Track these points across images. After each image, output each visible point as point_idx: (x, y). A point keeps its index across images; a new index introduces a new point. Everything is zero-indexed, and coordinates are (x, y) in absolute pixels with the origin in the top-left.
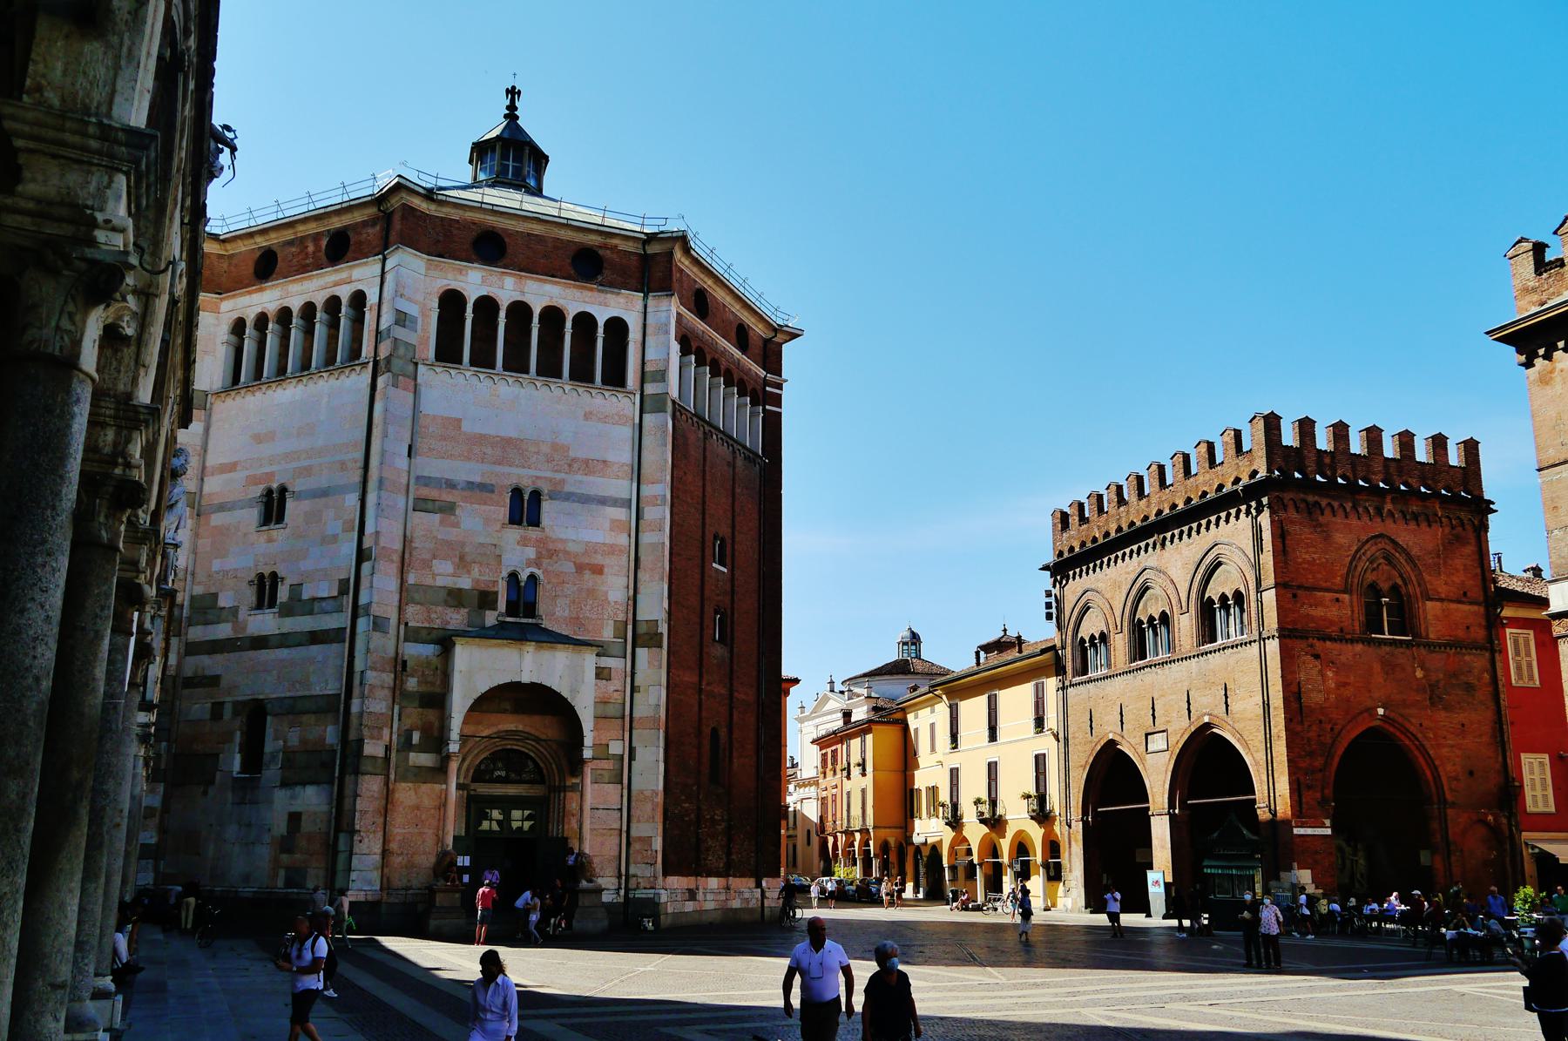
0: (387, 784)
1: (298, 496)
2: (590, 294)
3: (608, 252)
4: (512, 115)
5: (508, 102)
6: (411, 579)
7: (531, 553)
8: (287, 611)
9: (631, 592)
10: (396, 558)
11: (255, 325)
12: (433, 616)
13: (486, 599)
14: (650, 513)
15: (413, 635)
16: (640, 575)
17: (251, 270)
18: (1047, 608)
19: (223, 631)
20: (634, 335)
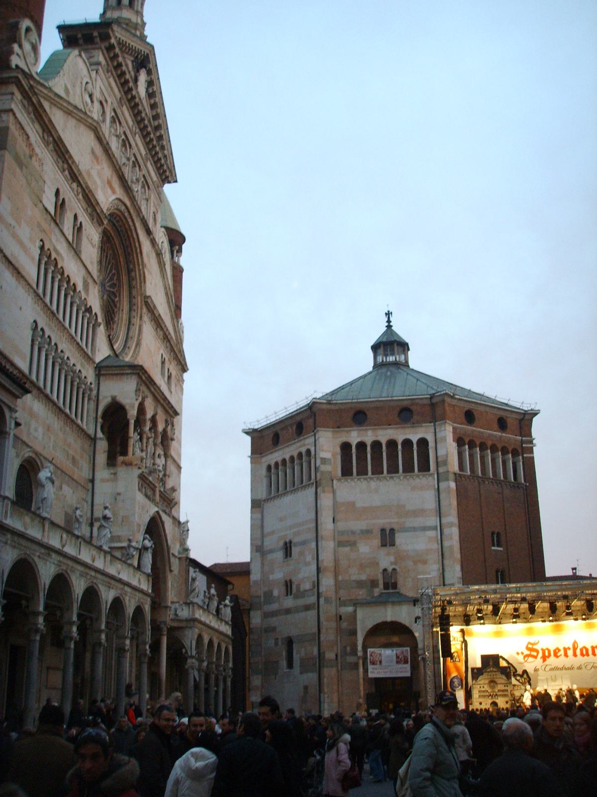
0: (338, 671)
2: (407, 429)
4: (389, 327)
5: (387, 319)
6: (340, 578)
7: (392, 559)
8: (296, 597)
9: (441, 571)
10: (333, 569)
13: (374, 583)
14: (446, 531)
15: (343, 603)
16: (445, 562)
17: (271, 442)
19: (275, 607)
20: (431, 444)
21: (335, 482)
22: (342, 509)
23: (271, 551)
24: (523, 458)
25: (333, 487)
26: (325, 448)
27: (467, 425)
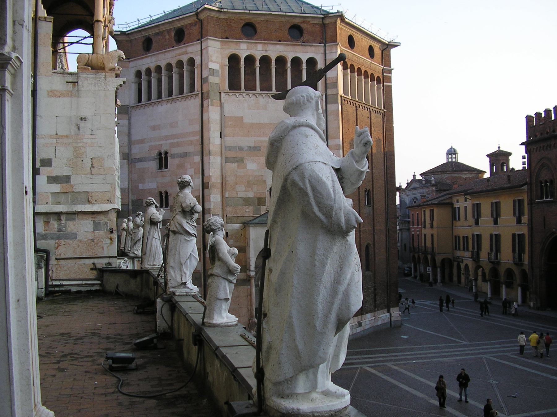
1: (173, 156)
2: (298, 47)
3: (305, 25)
6: (227, 195)
10: (220, 185)
11: (146, 73)
12: (238, 211)
13: (261, 201)
18: (523, 164)
21: (222, 94)
22: (230, 123)
23: (140, 160)
24: (383, 85)
25: (220, 100)
26: (214, 58)
27: (349, 50)
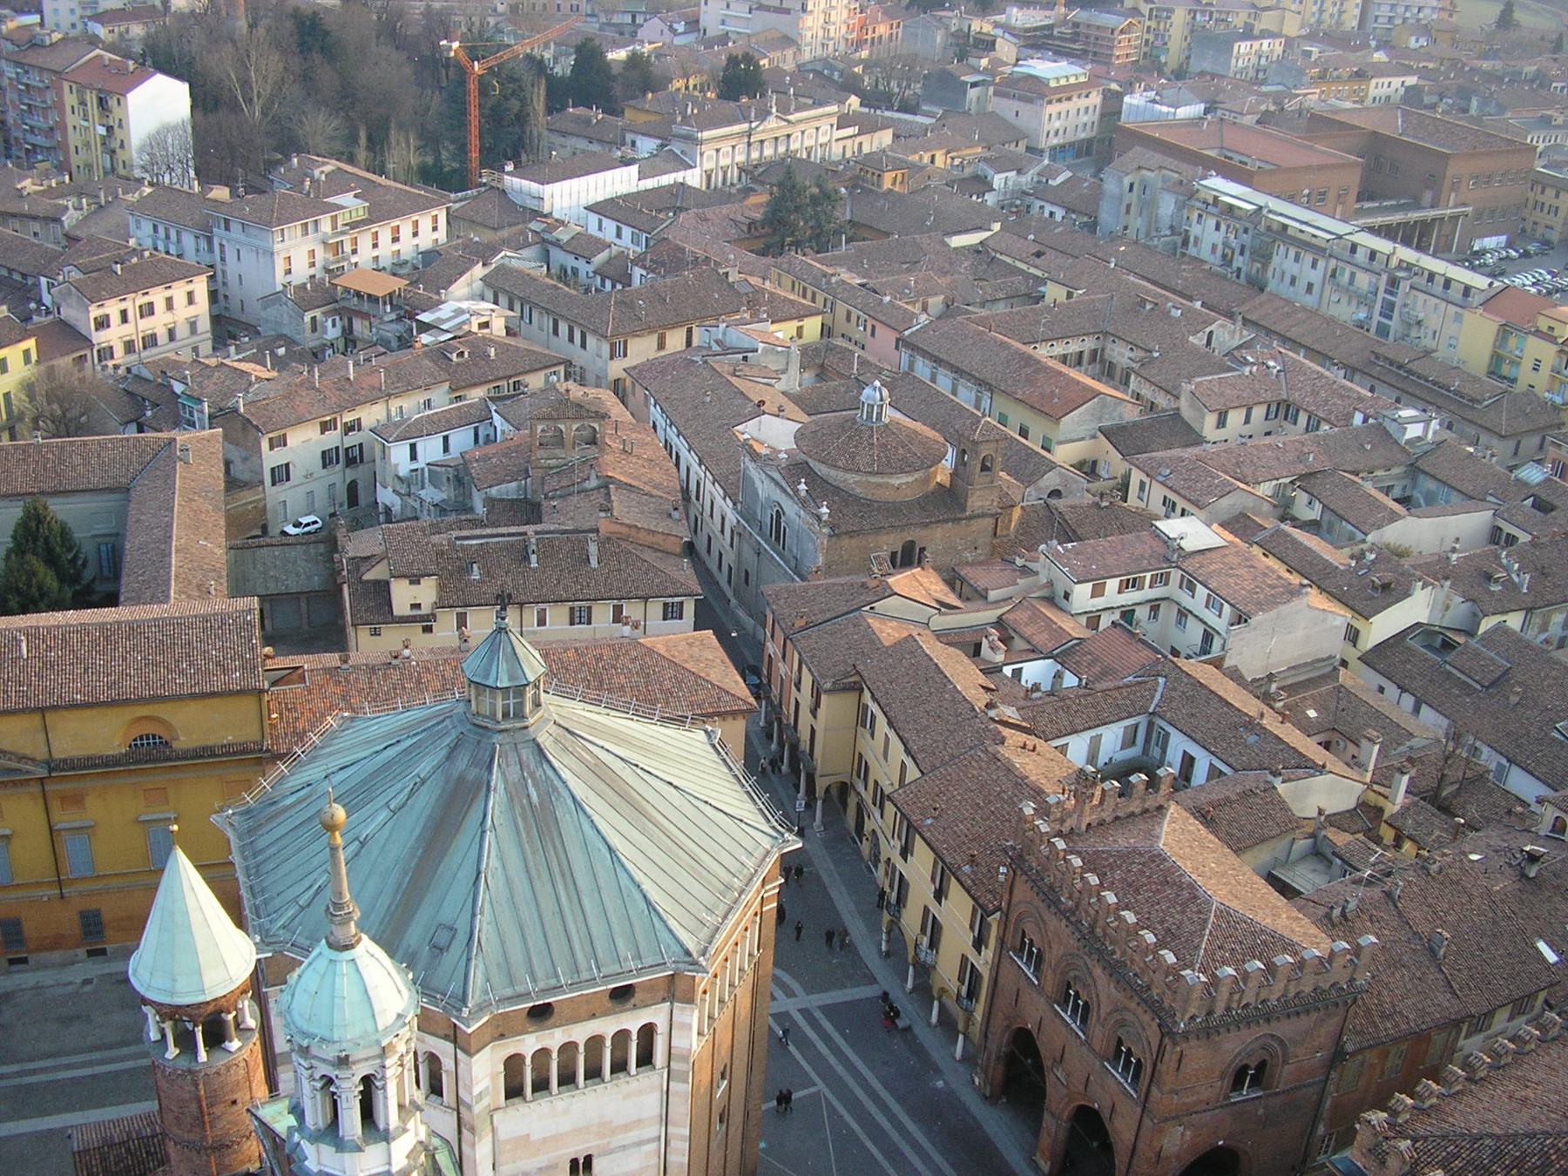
14: (673, 1143)
